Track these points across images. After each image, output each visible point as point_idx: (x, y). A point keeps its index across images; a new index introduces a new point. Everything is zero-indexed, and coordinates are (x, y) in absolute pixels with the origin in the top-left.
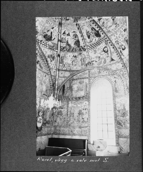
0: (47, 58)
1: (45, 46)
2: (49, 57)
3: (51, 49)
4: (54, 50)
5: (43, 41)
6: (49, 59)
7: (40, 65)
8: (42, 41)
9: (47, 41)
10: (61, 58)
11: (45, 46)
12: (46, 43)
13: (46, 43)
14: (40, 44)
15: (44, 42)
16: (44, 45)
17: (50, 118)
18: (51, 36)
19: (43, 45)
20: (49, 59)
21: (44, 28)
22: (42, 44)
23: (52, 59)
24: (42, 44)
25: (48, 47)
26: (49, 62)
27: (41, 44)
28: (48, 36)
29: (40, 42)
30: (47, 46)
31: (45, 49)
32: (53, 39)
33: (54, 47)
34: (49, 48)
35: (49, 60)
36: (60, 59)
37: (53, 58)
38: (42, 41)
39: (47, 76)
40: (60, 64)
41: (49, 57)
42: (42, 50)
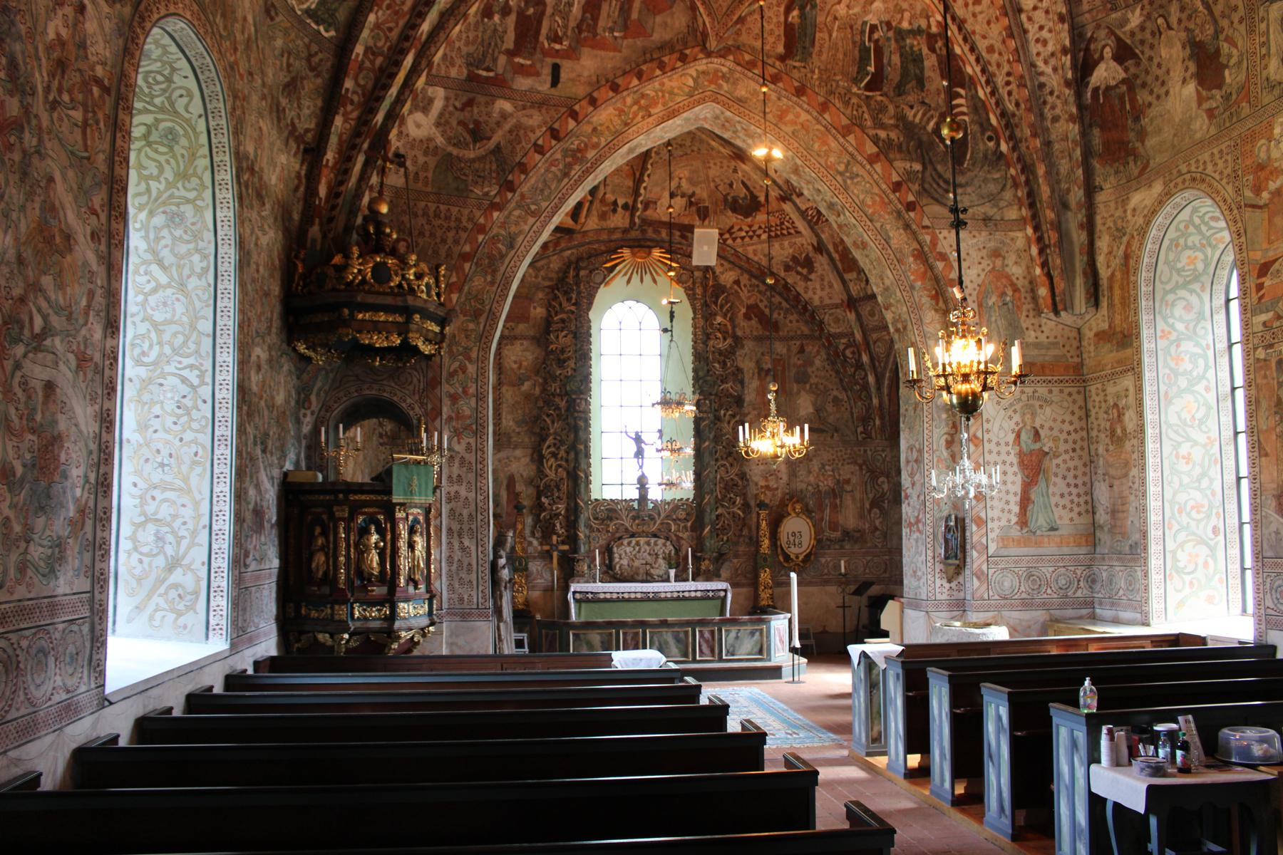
0: (782, 274)
1: (751, 237)
2: (787, 268)
3: (777, 236)
4: (789, 234)
5: (736, 228)
6: (793, 273)
7: (760, 322)
8: (732, 227)
9: (749, 219)
10: (837, 252)
11: (751, 237)
12: (750, 226)
13: (750, 226)
14: (730, 242)
15: (740, 229)
16: (747, 239)
17: (861, 516)
18: (751, 193)
19: (743, 238)
20: (793, 273)
21: (712, 185)
22: (739, 240)
23: (805, 271)
24: (739, 240)
25: (764, 237)
26: (800, 289)
27: (734, 239)
28: (743, 199)
29: (727, 236)
30: (759, 236)
31: (759, 247)
32: (762, 199)
33: (782, 223)
34: (770, 237)
35: (791, 279)
36: (836, 256)
37: (808, 264)
38: (732, 227)
39: (808, 349)
40: (847, 276)
41: (787, 268)
42: (751, 256)
